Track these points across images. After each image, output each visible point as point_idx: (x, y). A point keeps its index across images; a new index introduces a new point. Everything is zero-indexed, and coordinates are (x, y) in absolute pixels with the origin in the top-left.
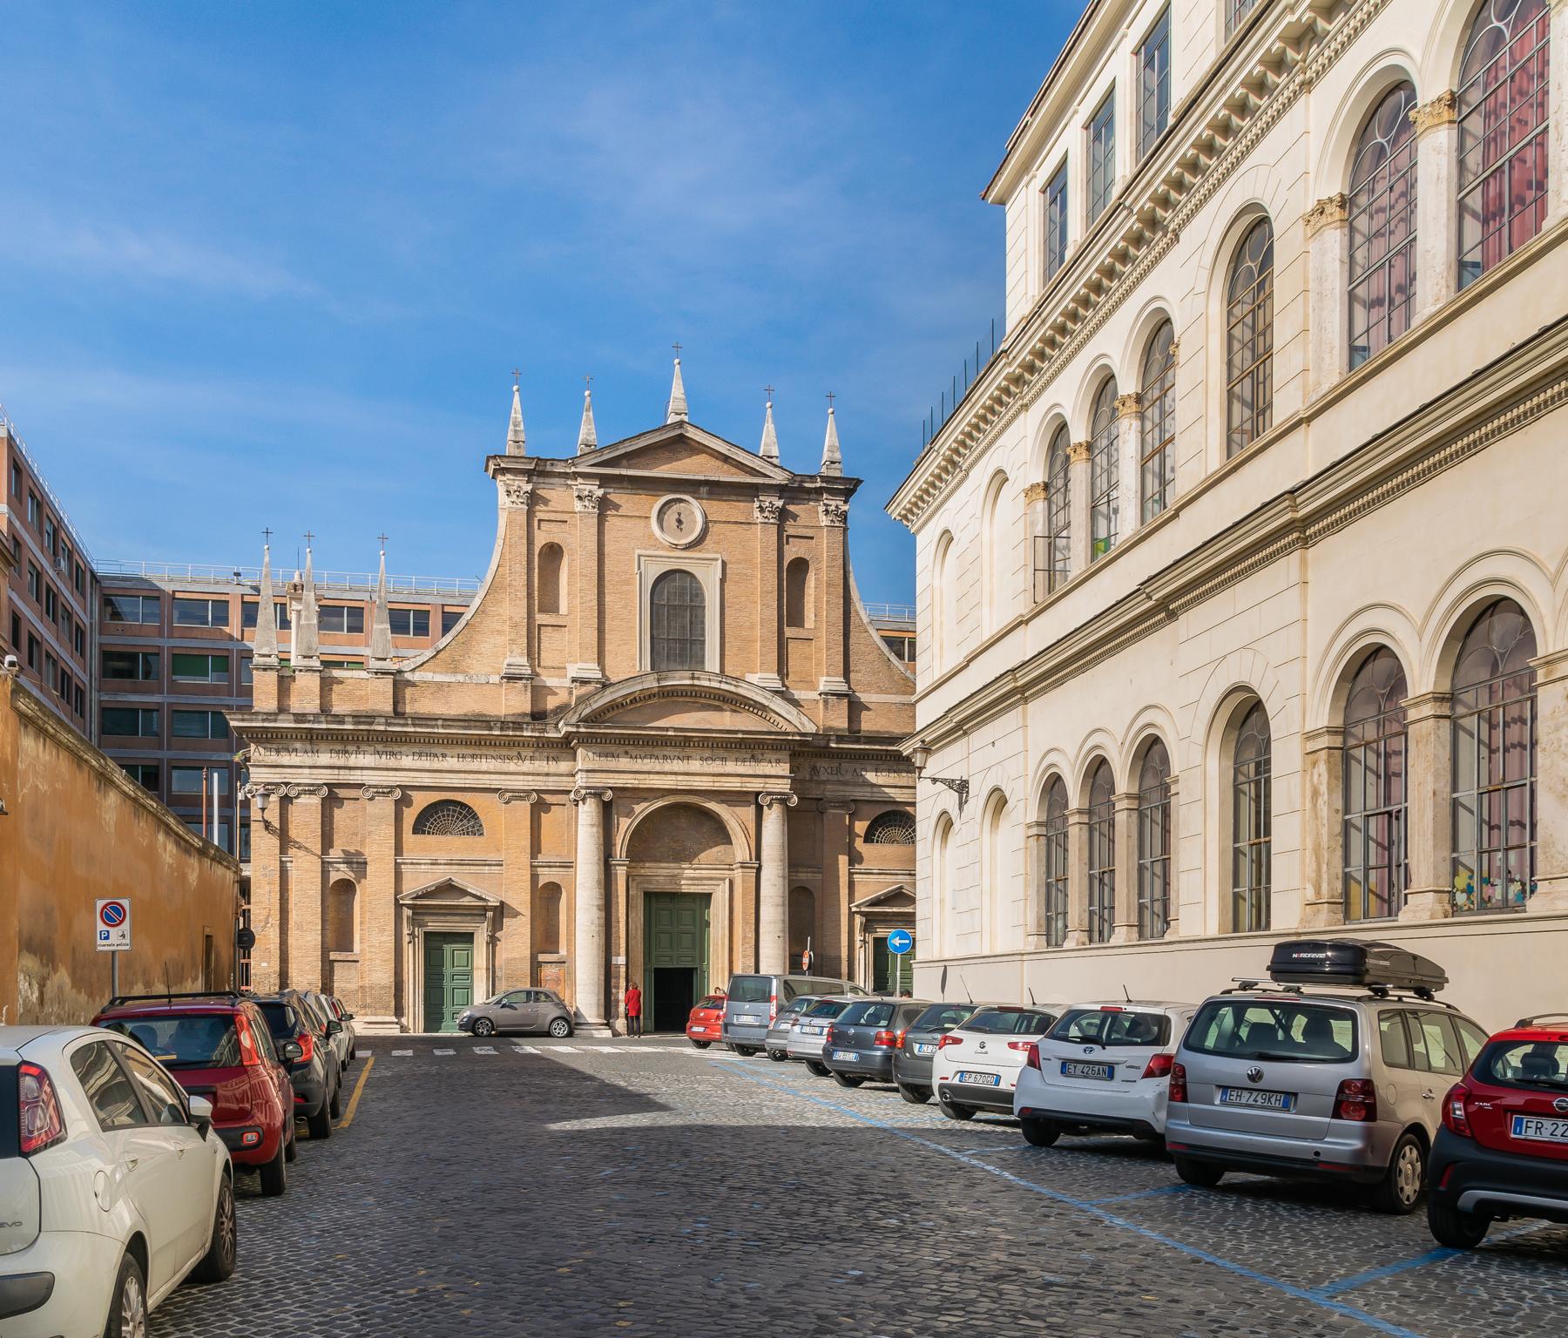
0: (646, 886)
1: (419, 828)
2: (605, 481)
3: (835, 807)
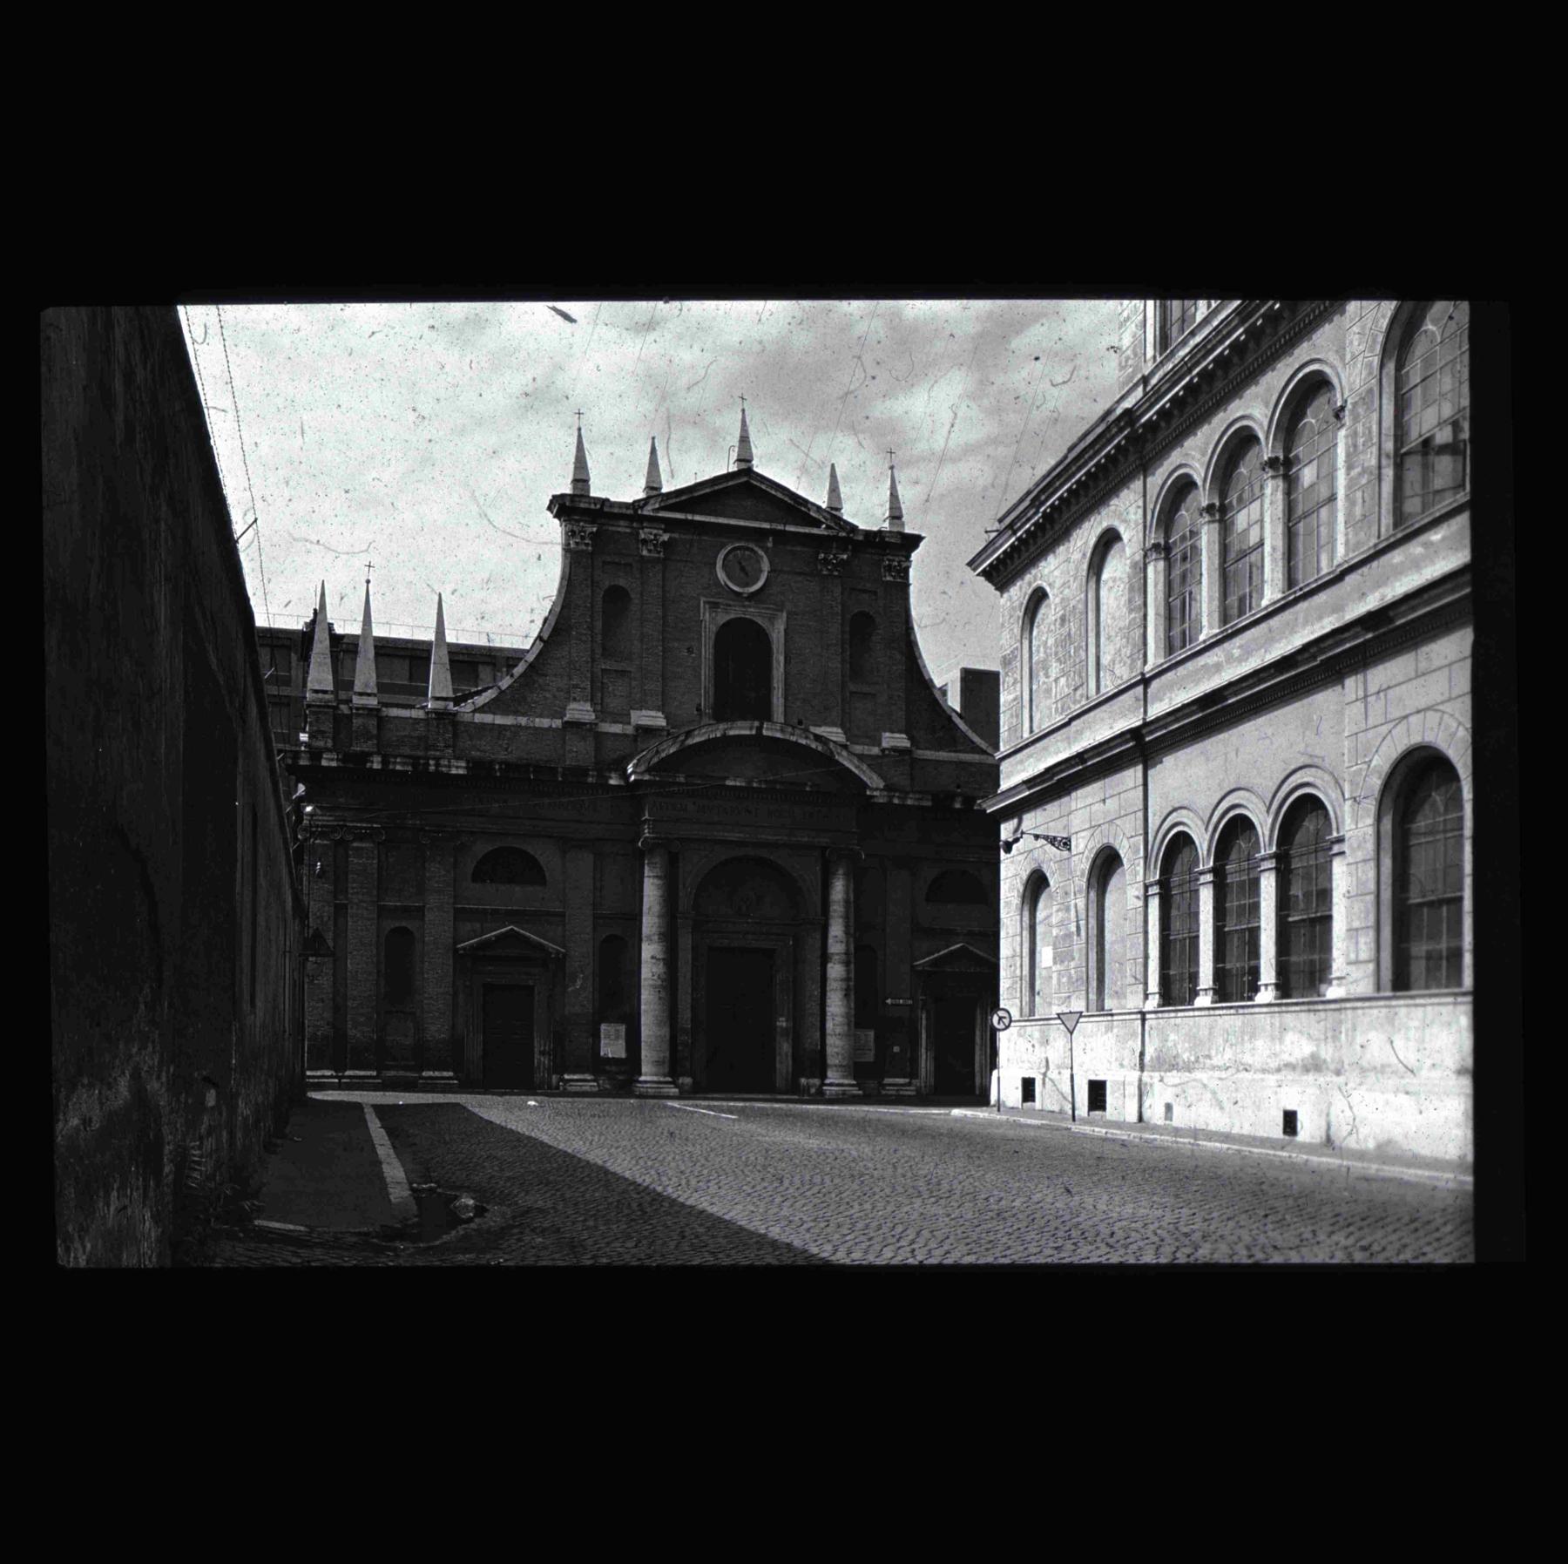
1: (478, 876)
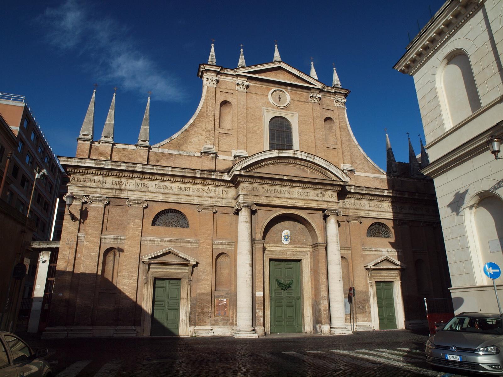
0: (270, 256)
2: (249, 78)
3: (354, 220)
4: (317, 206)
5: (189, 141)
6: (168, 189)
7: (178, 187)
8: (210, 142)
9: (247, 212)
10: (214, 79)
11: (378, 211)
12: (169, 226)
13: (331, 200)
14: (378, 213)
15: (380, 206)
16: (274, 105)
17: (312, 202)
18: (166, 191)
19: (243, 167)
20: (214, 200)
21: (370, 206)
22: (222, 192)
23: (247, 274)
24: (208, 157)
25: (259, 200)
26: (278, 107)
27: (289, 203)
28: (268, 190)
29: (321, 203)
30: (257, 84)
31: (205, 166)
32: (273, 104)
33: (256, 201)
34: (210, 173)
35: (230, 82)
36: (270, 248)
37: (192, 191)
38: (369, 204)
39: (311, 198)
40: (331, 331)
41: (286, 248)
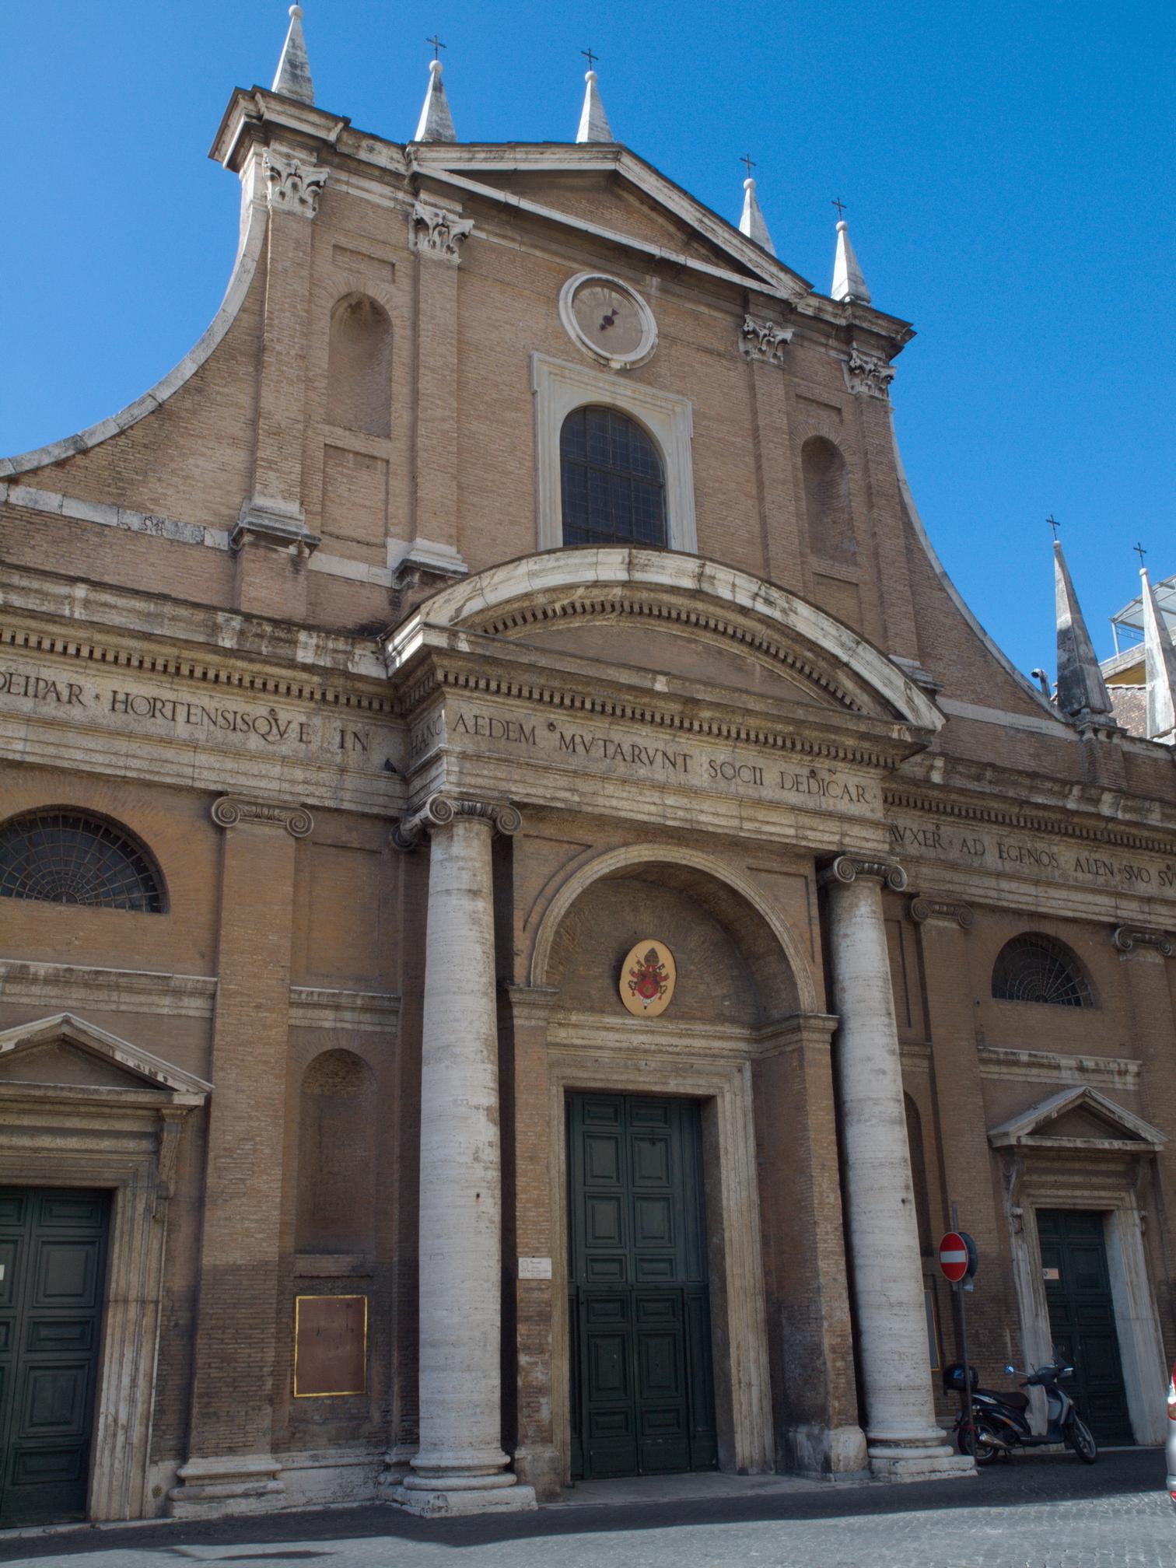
0: (569, 1072)
2: (473, 204)
4: (796, 837)
5: (174, 465)
6: (59, 699)
7: (115, 692)
8: (283, 486)
9: (476, 843)
10: (307, 181)
11: (1037, 883)
12: (57, 899)
13: (855, 809)
14: (1040, 889)
15: (1045, 859)
16: (584, 349)
17: (774, 817)
18: (50, 709)
19: (465, 613)
20: (299, 774)
21: (1005, 855)
22: (338, 739)
23: (476, 1159)
24: (274, 556)
25: (534, 785)
26: (602, 363)
27: (673, 809)
28: (578, 740)
29: (816, 822)
30: (504, 237)
31: (256, 599)
32: (579, 345)
33: (520, 791)
34: (288, 636)
35: (379, 206)
36: (571, 1032)
37: (188, 721)
38: (999, 845)
39: (769, 793)
40: (871, 1457)
41: (642, 1038)
